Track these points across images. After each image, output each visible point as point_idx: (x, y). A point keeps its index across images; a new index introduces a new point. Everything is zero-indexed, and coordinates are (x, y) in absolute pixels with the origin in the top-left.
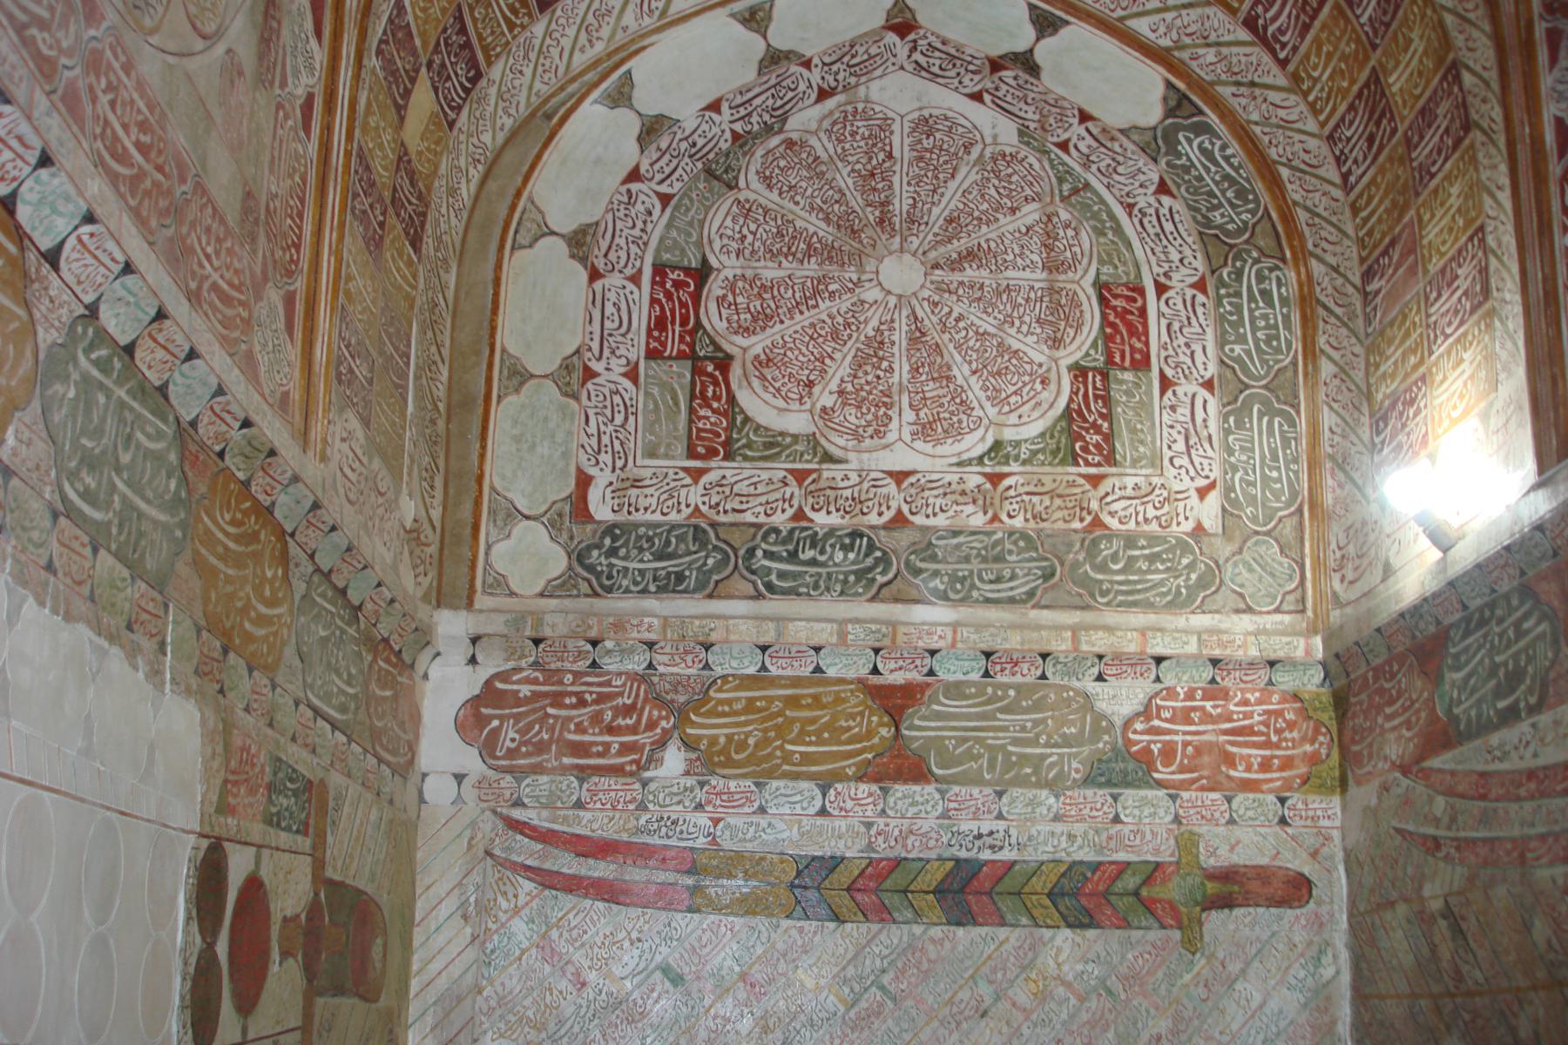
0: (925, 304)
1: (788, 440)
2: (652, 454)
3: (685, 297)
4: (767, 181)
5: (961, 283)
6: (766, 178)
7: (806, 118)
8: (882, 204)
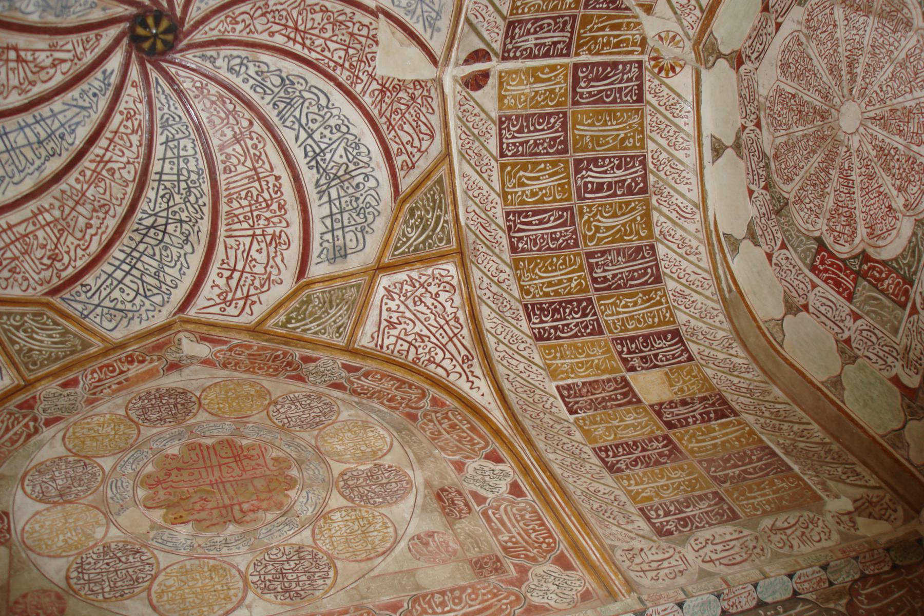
0: (869, 108)
1: (914, 239)
2: (895, 331)
3: (828, 261)
4: (789, 180)
5: (863, 78)
6: (787, 180)
7: (768, 140)
8: (815, 112)
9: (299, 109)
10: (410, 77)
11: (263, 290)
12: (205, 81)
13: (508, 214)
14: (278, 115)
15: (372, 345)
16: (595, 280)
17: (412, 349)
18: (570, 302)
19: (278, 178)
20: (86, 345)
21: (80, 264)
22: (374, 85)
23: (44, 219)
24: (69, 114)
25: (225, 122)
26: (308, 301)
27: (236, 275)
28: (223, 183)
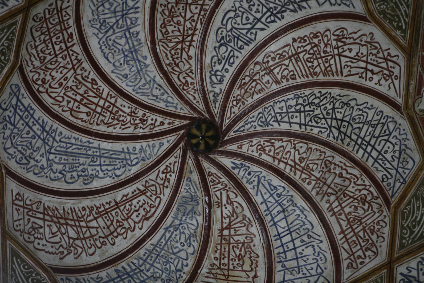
9: (241, 31)
11: (379, 47)
12: (231, 98)
14: (248, 45)
19: (294, 40)
21: (368, 182)
23: (337, 207)
24: (264, 191)
25: (258, 81)
26: (383, 12)
27: (370, 67)
28: (303, 79)
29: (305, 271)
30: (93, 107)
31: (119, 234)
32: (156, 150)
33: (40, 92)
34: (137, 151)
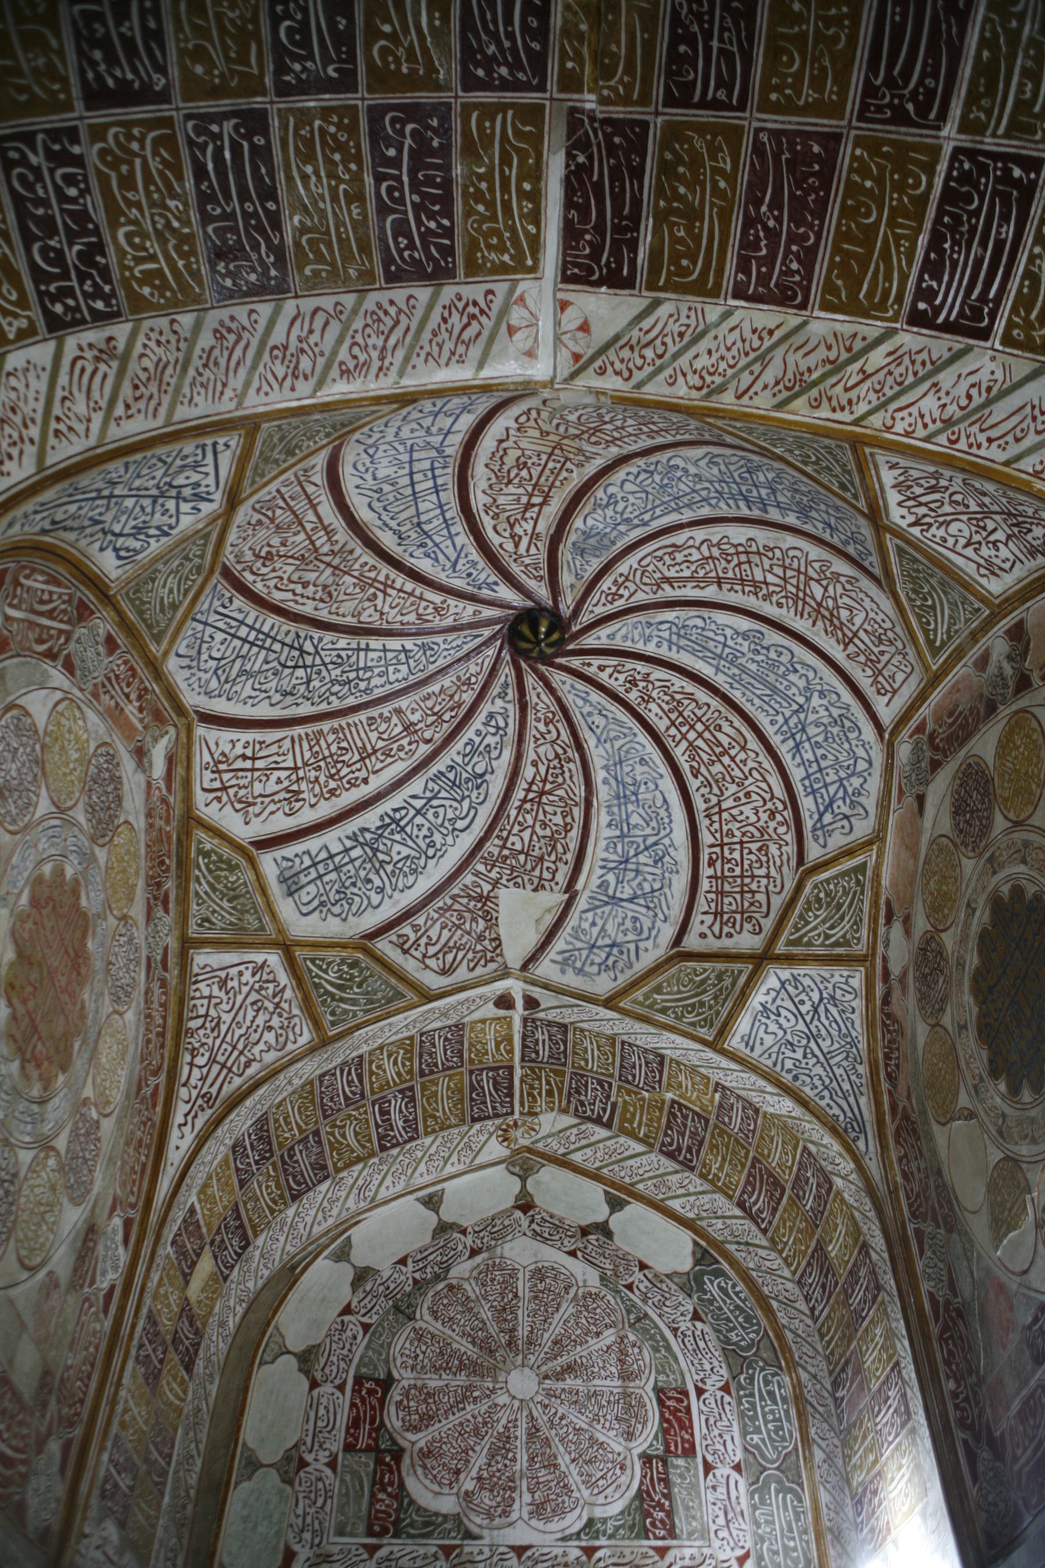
3: (375, 1402)
7: (462, 1269)
10: (502, 931)
12: (478, 688)
13: (361, 1057)
15: (196, 970)
16: (292, 1148)
17: (200, 1021)
18: (270, 1143)
20: (158, 638)
21: (259, 588)
22: (487, 888)
26: (232, 868)
27: (248, 764)
29: (401, 448)
30: (707, 735)
31: (735, 546)
32: (623, 631)
33: (783, 803)
34: (655, 640)
